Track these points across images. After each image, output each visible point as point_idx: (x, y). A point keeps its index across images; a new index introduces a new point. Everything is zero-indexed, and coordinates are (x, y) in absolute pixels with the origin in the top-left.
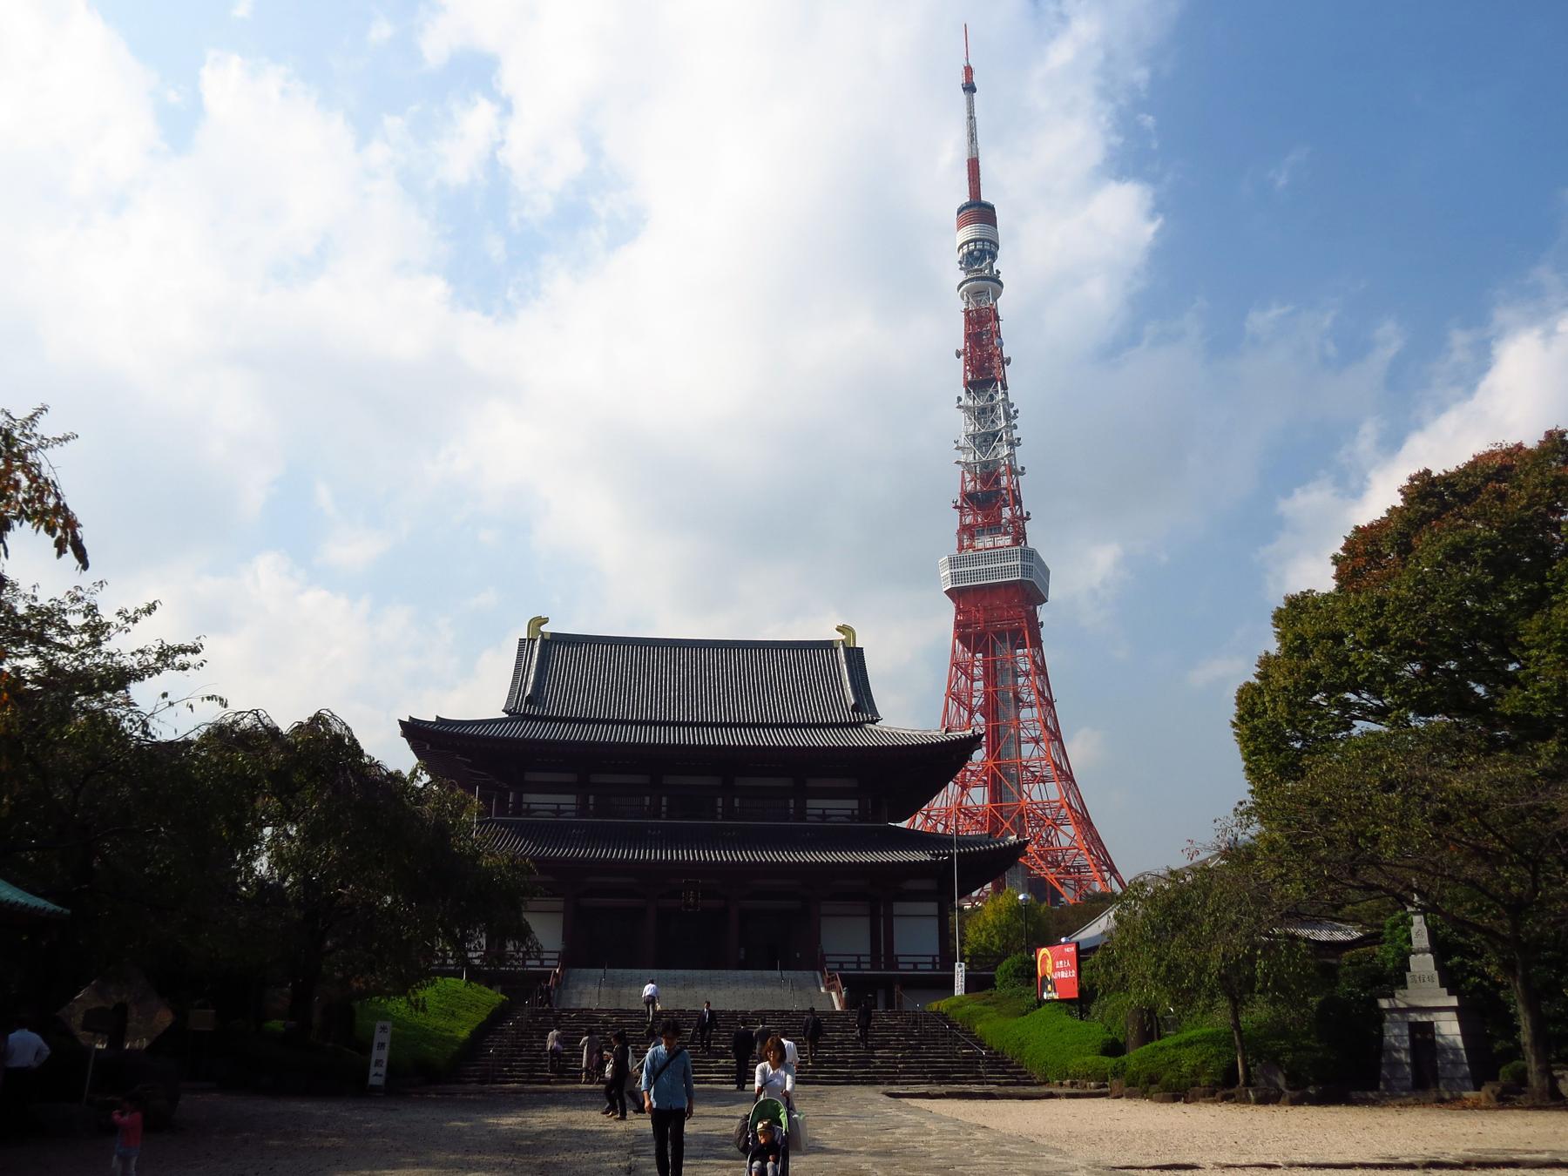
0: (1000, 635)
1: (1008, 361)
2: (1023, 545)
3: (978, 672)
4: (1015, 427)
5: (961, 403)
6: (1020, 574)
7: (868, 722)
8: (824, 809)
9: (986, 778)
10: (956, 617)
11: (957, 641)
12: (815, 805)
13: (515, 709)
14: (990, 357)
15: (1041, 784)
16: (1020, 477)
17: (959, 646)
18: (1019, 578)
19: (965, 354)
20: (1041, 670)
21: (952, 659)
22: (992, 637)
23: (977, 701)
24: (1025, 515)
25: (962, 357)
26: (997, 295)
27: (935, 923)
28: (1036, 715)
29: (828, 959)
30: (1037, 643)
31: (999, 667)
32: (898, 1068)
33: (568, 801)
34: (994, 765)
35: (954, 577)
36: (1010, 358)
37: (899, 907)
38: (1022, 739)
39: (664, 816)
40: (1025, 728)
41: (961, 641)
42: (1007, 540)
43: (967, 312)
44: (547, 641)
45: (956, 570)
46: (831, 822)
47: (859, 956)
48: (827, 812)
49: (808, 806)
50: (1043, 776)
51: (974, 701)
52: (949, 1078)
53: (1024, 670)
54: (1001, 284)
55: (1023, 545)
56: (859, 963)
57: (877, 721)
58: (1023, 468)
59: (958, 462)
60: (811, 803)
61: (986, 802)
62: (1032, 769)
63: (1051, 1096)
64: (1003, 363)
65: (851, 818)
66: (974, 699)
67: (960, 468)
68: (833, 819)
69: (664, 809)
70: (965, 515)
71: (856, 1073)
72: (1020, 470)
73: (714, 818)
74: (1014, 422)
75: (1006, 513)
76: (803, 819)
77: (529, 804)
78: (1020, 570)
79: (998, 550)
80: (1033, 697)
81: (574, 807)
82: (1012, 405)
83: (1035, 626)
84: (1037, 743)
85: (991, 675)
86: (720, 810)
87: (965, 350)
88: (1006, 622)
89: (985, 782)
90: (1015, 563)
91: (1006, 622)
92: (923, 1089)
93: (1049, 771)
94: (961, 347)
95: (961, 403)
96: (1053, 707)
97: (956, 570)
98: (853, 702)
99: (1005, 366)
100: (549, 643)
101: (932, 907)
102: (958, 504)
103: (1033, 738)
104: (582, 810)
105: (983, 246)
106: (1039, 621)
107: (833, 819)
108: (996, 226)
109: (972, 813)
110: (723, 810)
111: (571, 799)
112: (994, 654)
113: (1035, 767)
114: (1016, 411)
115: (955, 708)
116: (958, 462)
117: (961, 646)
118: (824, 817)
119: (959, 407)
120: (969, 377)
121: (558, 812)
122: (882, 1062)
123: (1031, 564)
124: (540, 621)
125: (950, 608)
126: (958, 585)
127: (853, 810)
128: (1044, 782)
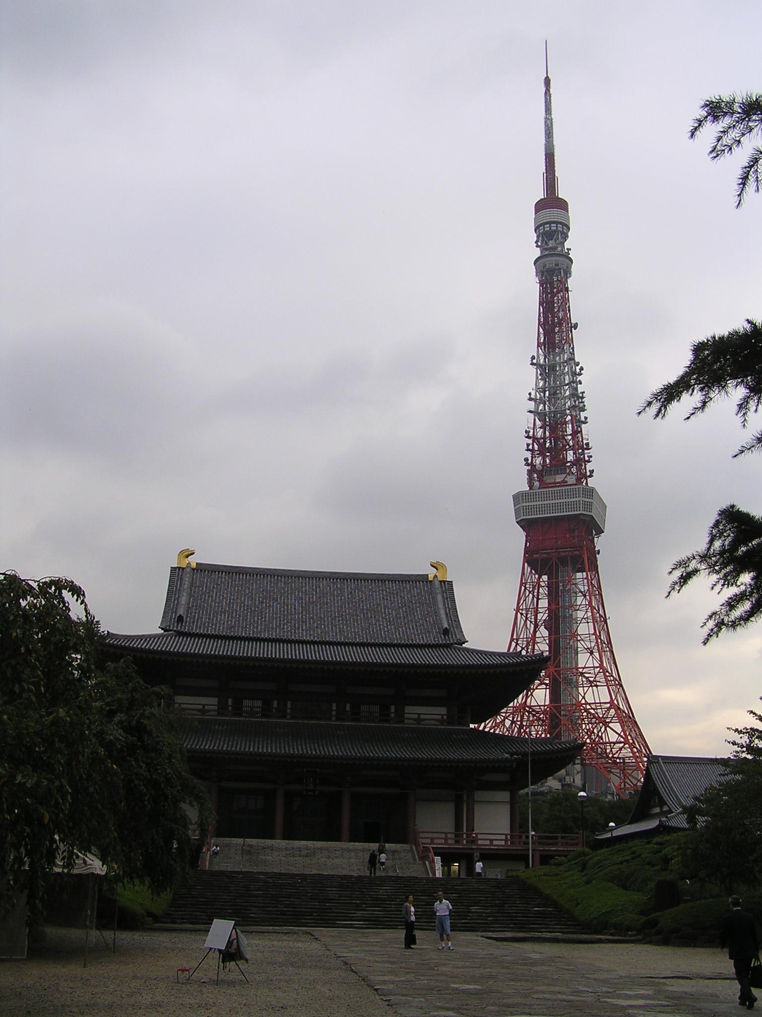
0: (563, 561)
1: (576, 326)
2: (584, 484)
3: (543, 591)
4: (581, 383)
5: (535, 361)
7: (456, 644)
8: (419, 714)
9: (547, 682)
10: (526, 544)
11: (526, 564)
12: (412, 711)
13: (169, 626)
14: (560, 324)
15: (595, 688)
17: (528, 569)
20: (596, 592)
21: (522, 580)
22: (556, 564)
23: (543, 616)
24: (587, 459)
27: (507, 808)
28: (592, 631)
29: (421, 835)
30: (594, 567)
31: (561, 588)
32: (487, 920)
33: (211, 702)
34: (555, 671)
36: (577, 323)
37: (479, 795)
38: (579, 649)
39: (288, 716)
40: (582, 640)
41: (529, 565)
42: (571, 480)
44: (194, 569)
46: (424, 725)
47: (446, 833)
48: (422, 716)
49: (406, 712)
50: (596, 681)
51: (539, 616)
52: (525, 928)
53: (582, 590)
54: (572, 262)
55: (584, 484)
56: (446, 839)
57: (464, 643)
58: (586, 418)
59: (530, 412)
60: (408, 709)
61: (547, 703)
62: (587, 675)
63: (600, 941)
64: (571, 327)
65: (441, 722)
66: (539, 615)
67: (532, 415)
68: (426, 722)
69: (289, 711)
70: (535, 457)
71: (458, 923)
72: (583, 419)
73: (330, 719)
74: (579, 378)
75: (570, 456)
76: (402, 722)
77: (180, 704)
79: (563, 488)
80: (589, 614)
81: (216, 708)
82: (578, 364)
83: (593, 554)
84: (592, 653)
85: (554, 595)
86: (334, 713)
88: (569, 549)
89: (546, 684)
90: (577, 499)
91: (569, 549)
92: (509, 935)
93: (601, 678)
95: (535, 361)
96: (606, 623)
98: (446, 625)
99: (573, 329)
100: (196, 571)
101: (505, 796)
102: (531, 447)
103: (588, 648)
104: (222, 709)
105: (557, 227)
106: (597, 549)
107: (426, 722)
108: (567, 211)
109: (534, 710)
110: (337, 713)
111: (214, 701)
112: (557, 578)
113: (590, 673)
114: (582, 369)
115: (523, 622)
116: (530, 412)
117: (529, 570)
118: (419, 720)
119: (532, 364)
121: (203, 711)
122: (477, 916)
123: (591, 500)
124: (190, 553)
125: (520, 537)
127: (442, 715)
128: (597, 686)
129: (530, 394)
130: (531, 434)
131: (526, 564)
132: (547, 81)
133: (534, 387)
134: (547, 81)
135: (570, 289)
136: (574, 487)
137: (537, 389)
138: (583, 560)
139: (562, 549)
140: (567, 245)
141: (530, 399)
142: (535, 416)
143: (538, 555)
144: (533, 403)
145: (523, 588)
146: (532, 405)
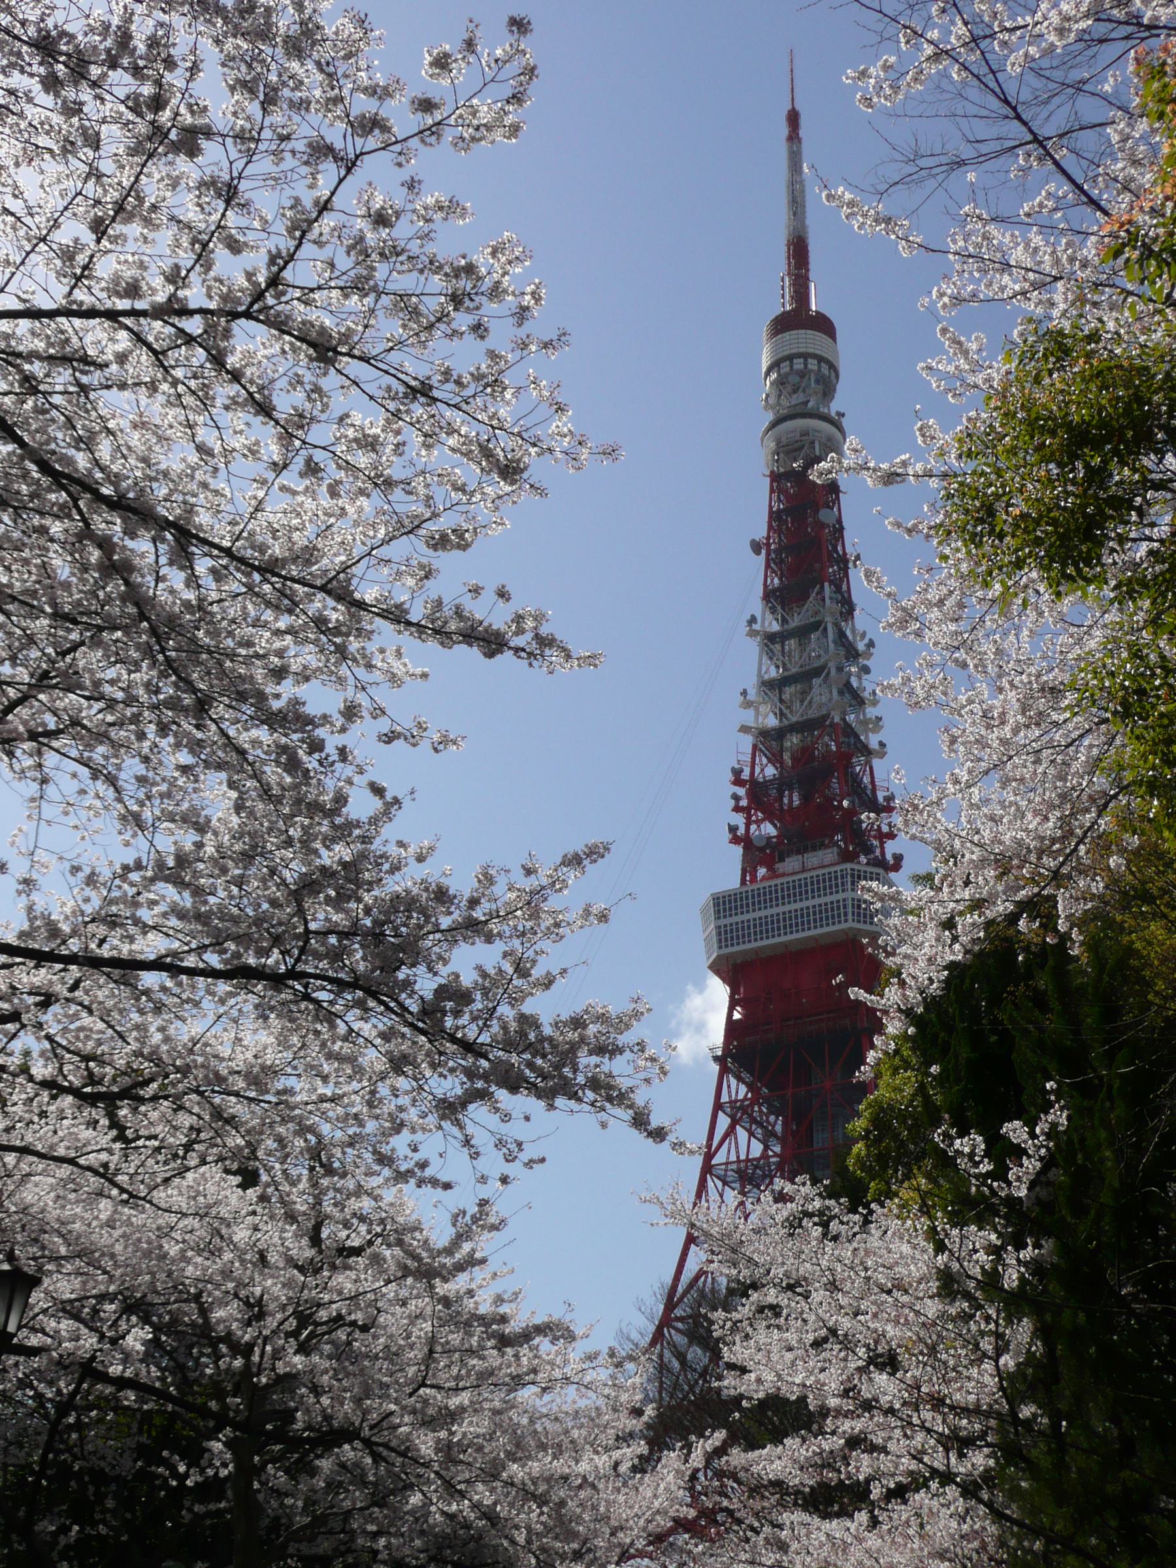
6: (850, 917)
18: (850, 924)
25: (764, 552)
35: (724, 935)
45: (728, 921)
58: (882, 745)
59: (744, 729)
78: (850, 910)
87: (768, 538)
90: (841, 896)
97: (728, 921)
108: (834, 339)
116: (744, 729)
126: (730, 950)
129: (744, 693)
130: (746, 775)
132: (793, 118)
134: (793, 118)
136: (832, 869)
140: (835, 407)
141: (747, 704)
144: (751, 712)
145: (723, 1122)
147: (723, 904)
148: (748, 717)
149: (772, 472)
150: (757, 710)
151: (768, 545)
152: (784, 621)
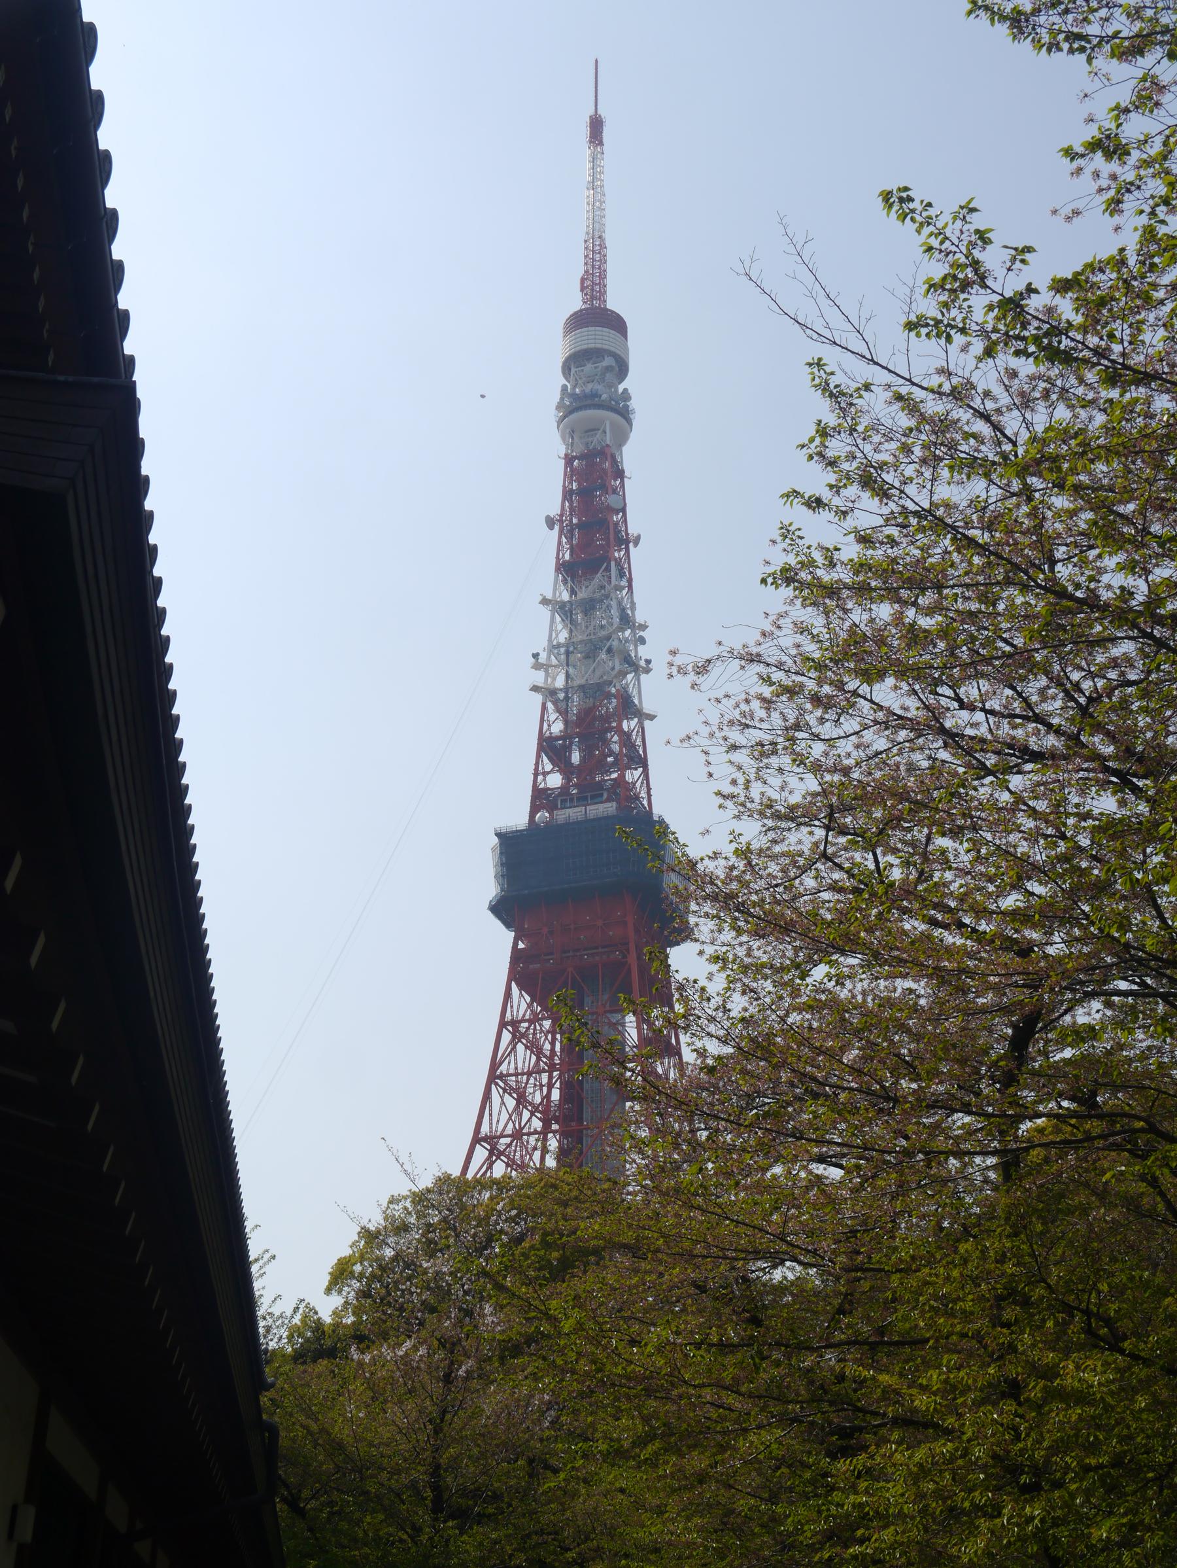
1: (637, 541)
4: (642, 641)
10: (515, 944)
11: (513, 984)
16: (647, 723)
19: (561, 521)
25: (557, 528)
26: (622, 438)
41: (521, 987)
43: (569, 460)
54: (629, 422)
59: (535, 689)
67: (538, 698)
87: (561, 515)
94: (555, 510)
99: (631, 545)
116: (535, 689)
120: (567, 557)
129: (536, 656)
131: (513, 984)
132: (596, 126)
133: (545, 644)
134: (596, 126)
135: (627, 474)
137: (553, 648)
138: (629, 972)
139: (585, 949)
141: (537, 666)
142: (545, 697)
143: (538, 966)
145: (506, 1037)
146: (539, 678)
147: (509, 843)
148: (539, 678)
149: (566, 455)
150: (546, 671)
151: (561, 521)
152: (573, 592)
